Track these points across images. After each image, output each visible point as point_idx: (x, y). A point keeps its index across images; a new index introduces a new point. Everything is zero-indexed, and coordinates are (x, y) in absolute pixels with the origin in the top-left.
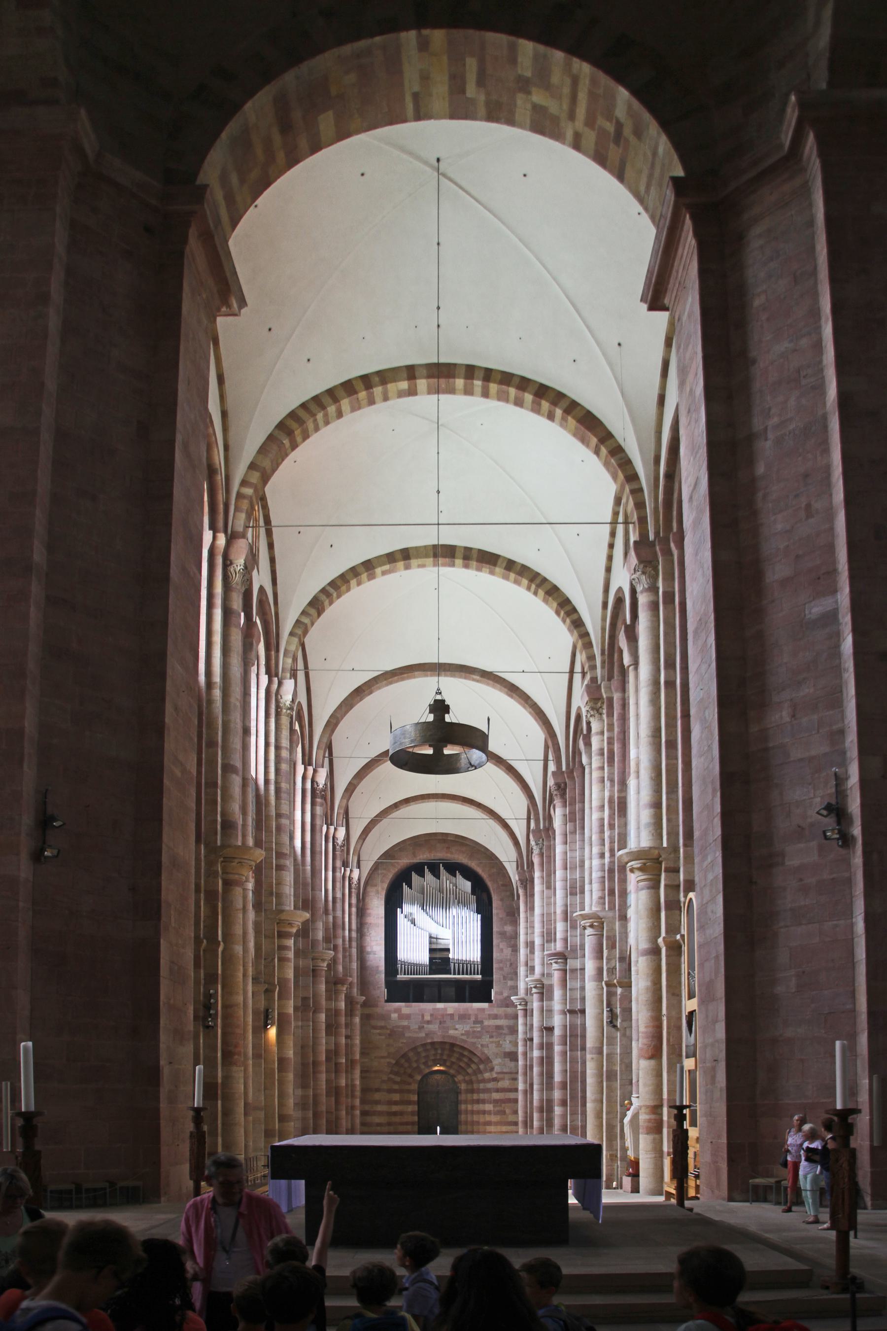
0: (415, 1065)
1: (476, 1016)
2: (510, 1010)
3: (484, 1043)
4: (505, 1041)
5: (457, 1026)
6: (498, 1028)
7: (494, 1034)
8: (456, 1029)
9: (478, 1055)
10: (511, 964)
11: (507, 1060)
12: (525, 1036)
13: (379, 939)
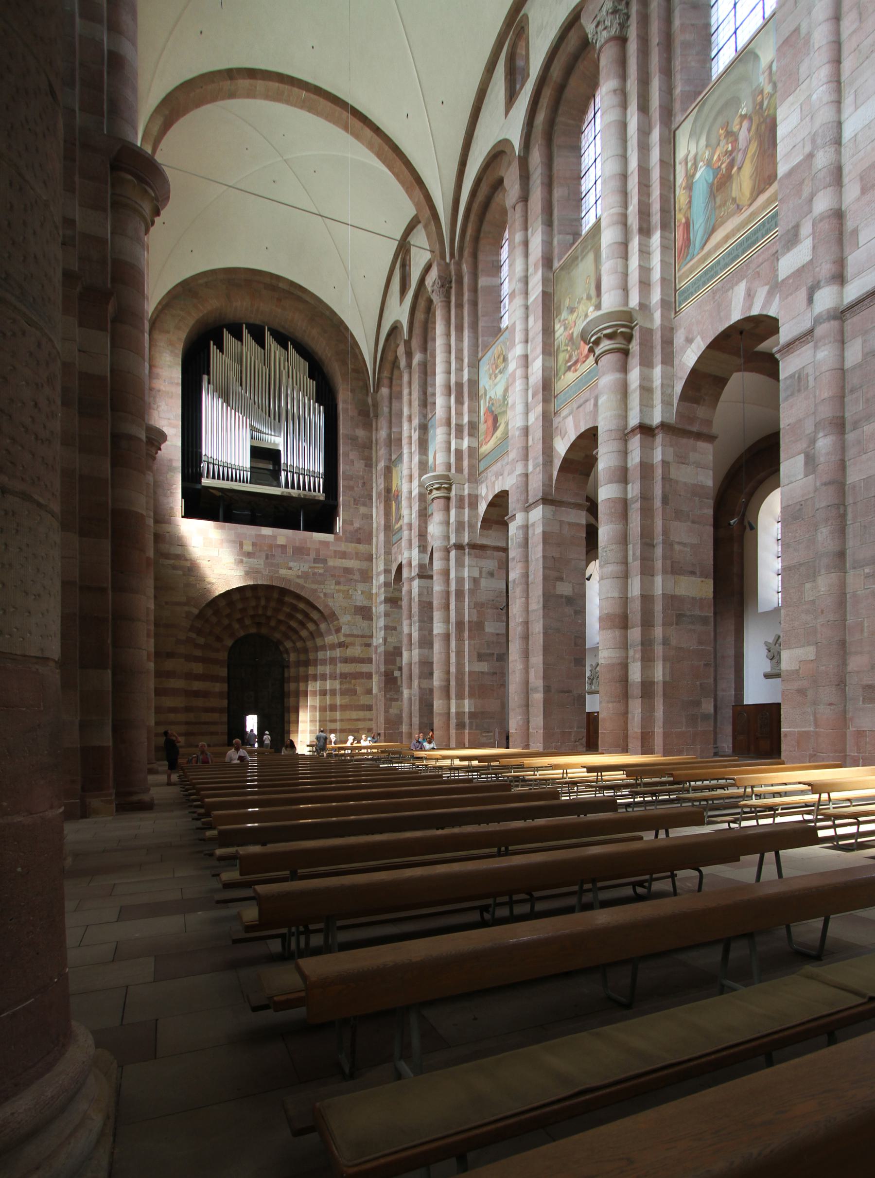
0: (226, 622)
1: (318, 551)
2: (362, 548)
3: (328, 591)
4: (356, 590)
5: (291, 564)
6: (347, 571)
7: (342, 579)
8: (290, 568)
9: (321, 608)
10: (364, 483)
11: (359, 618)
12: (445, 544)
13: (172, 417)
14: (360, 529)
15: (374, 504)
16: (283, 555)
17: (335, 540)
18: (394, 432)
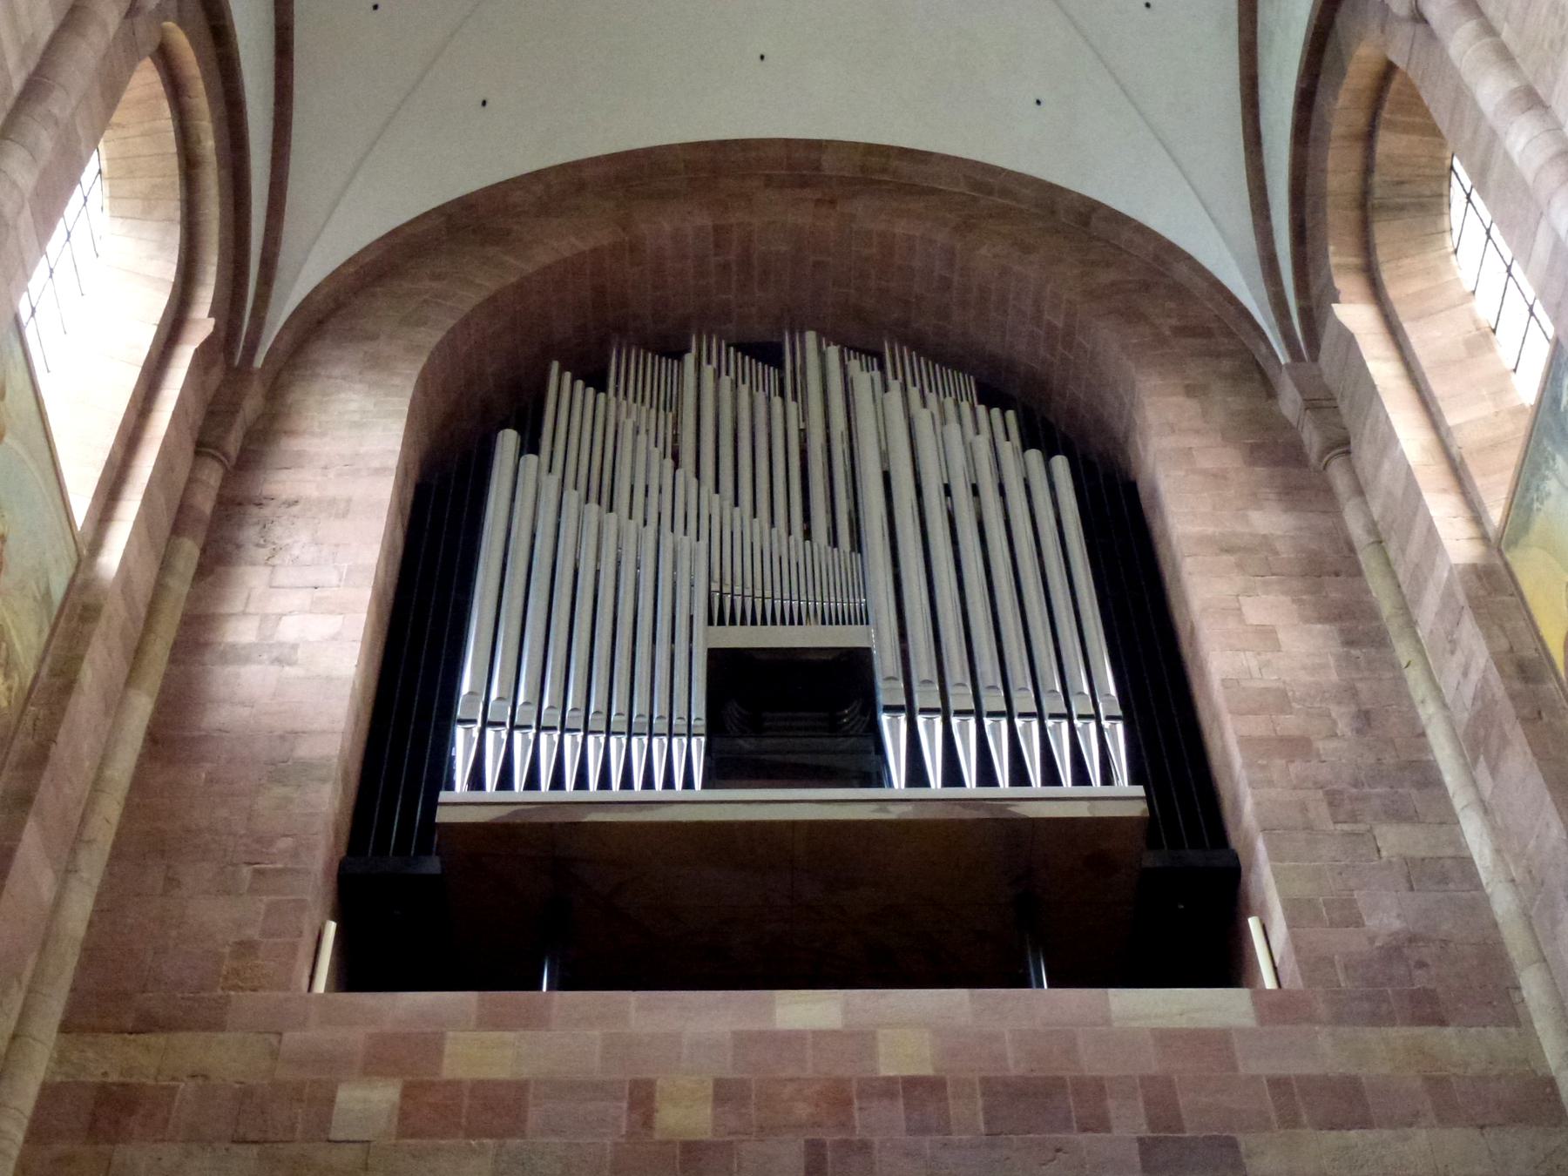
14: (1413, 939)
15: (1460, 798)
16: (926, 1141)
17: (1262, 1020)
18: (1459, 426)
